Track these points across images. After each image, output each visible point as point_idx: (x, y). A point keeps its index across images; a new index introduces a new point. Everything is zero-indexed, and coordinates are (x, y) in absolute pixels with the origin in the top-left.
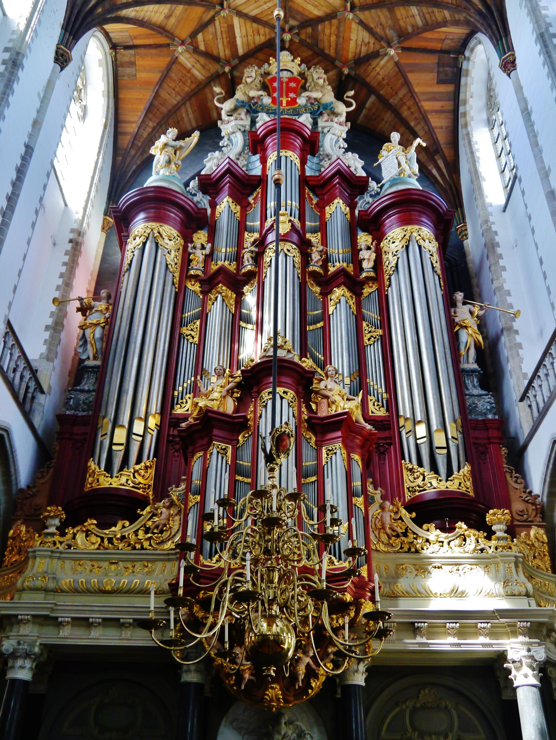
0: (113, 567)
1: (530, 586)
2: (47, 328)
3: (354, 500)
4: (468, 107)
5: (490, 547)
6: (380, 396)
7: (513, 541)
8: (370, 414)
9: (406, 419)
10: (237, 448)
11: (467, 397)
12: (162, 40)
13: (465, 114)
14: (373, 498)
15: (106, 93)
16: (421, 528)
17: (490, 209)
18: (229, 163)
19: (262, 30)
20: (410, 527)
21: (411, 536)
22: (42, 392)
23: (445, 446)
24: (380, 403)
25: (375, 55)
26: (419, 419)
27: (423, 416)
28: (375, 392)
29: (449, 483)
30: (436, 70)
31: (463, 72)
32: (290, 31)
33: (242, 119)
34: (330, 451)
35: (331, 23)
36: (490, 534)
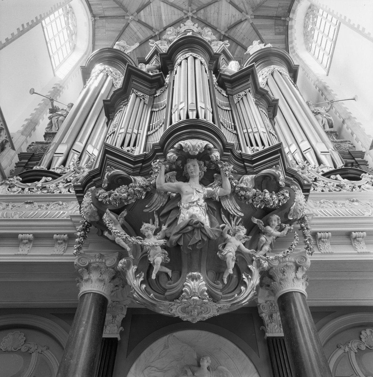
0: (27, 206)
2: (26, 120)
4: (294, 44)
10: (154, 97)
12: (120, 12)
13: (293, 48)
15: (88, 39)
17: (318, 75)
18: (156, 47)
19: (176, 11)
22: (13, 148)
25: (240, 22)
30: (274, 28)
31: (289, 27)
32: (191, 12)
33: (165, 45)
34: (240, 95)
35: (214, 5)
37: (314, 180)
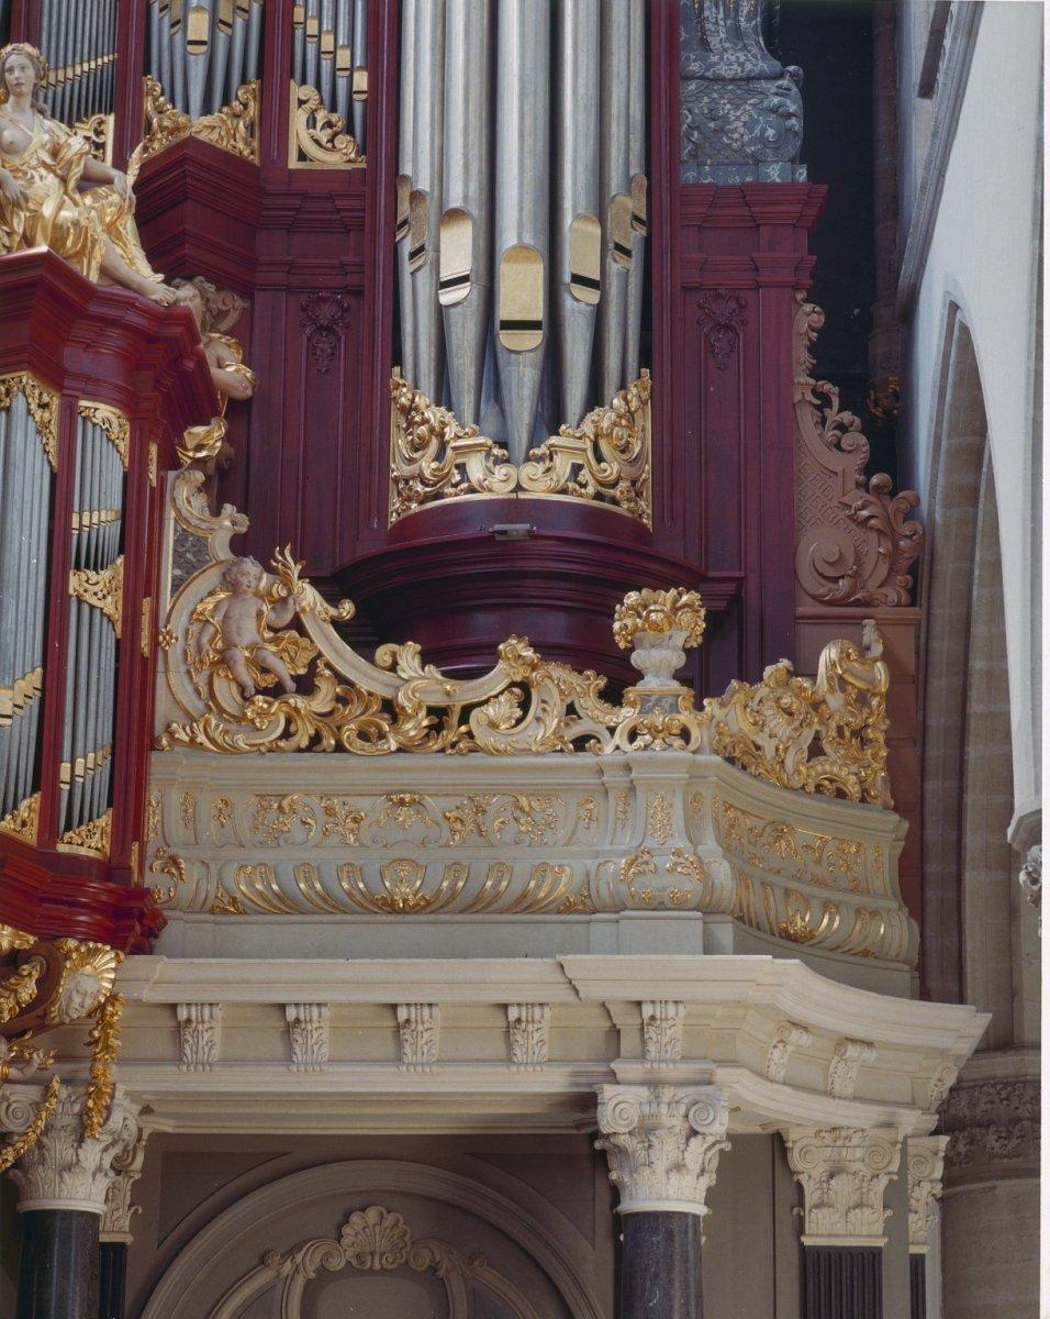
1: (722, 872)
3: (75, 582)
5: (612, 730)
6: (342, 83)
7: (699, 707)
8: (293, 163)
9: (417, 196)
11: (692, 86)
14: (201, 546)
16: (371, 659)
20: (329, 656)
21: (326, 690)
23: (538, 314)
24: (338, 118)
26: (455, 200)
27: (474, 186)
28: (326, 65)
29: (532, 470)
36: (619, 679)
37: (302, 671)
